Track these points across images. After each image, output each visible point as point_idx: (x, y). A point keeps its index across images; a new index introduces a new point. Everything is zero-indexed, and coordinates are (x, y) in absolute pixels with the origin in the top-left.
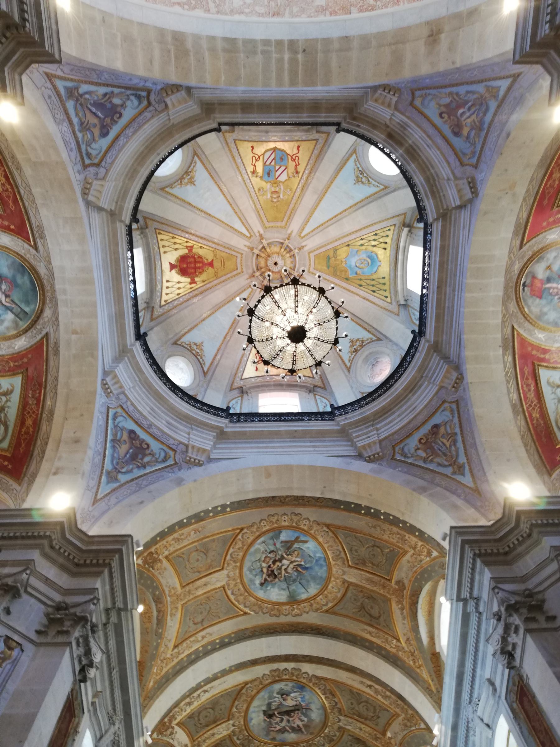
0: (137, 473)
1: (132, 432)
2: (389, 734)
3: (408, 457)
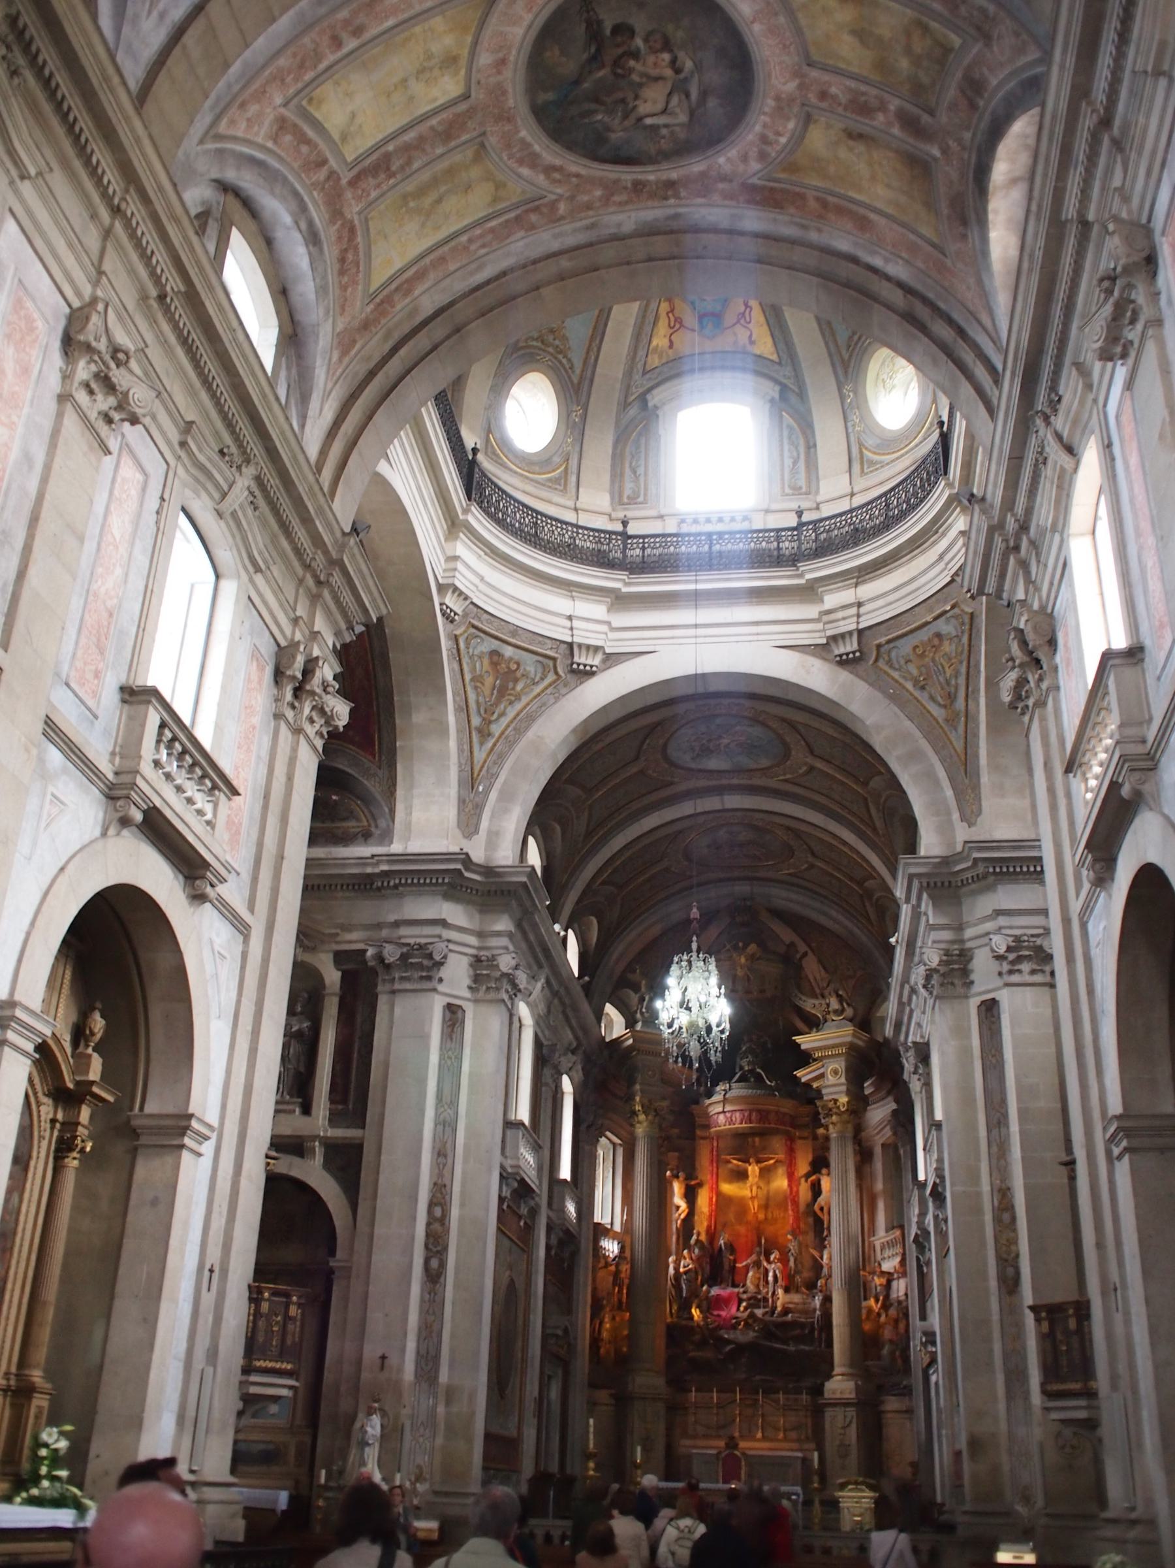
0: (511, 712)
1: (494, 653)
2: (866, 884)
3: (895, 669)
